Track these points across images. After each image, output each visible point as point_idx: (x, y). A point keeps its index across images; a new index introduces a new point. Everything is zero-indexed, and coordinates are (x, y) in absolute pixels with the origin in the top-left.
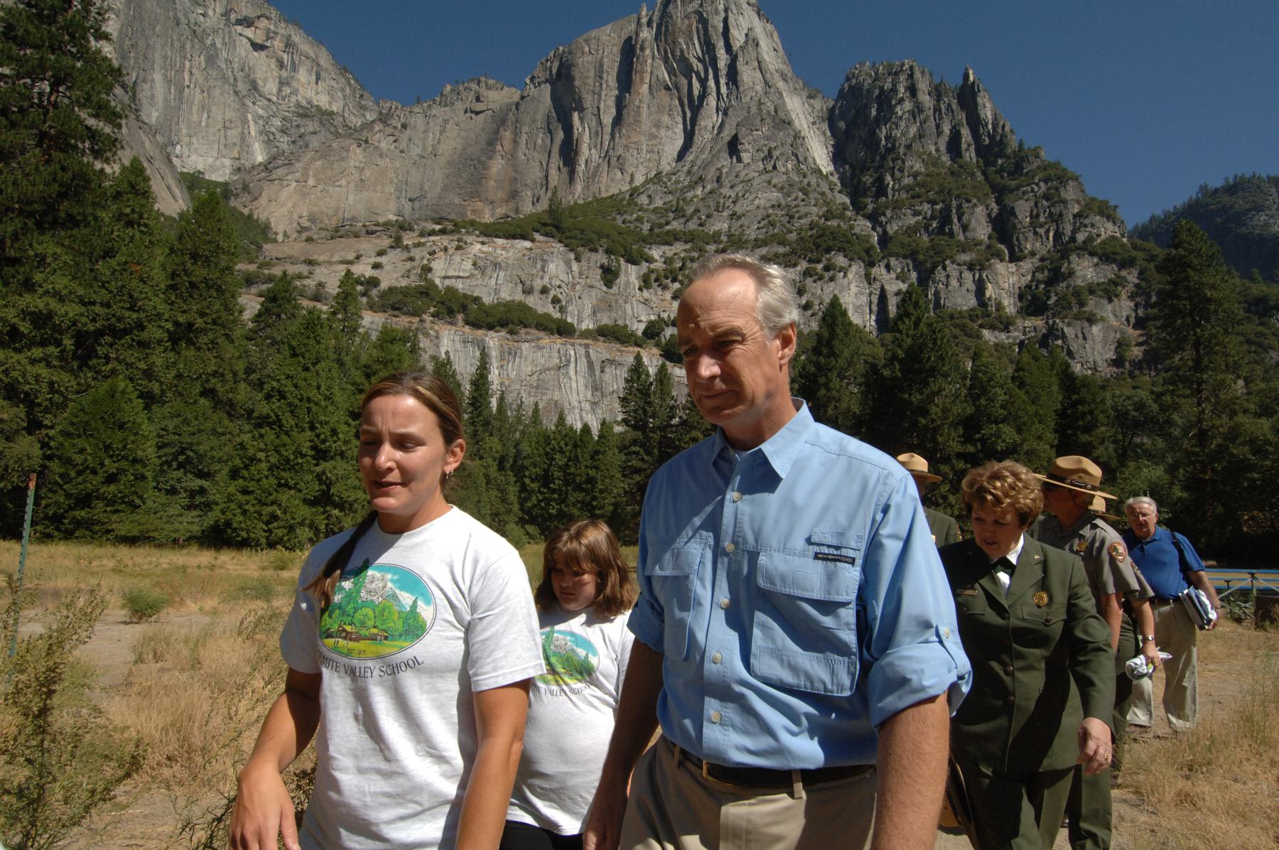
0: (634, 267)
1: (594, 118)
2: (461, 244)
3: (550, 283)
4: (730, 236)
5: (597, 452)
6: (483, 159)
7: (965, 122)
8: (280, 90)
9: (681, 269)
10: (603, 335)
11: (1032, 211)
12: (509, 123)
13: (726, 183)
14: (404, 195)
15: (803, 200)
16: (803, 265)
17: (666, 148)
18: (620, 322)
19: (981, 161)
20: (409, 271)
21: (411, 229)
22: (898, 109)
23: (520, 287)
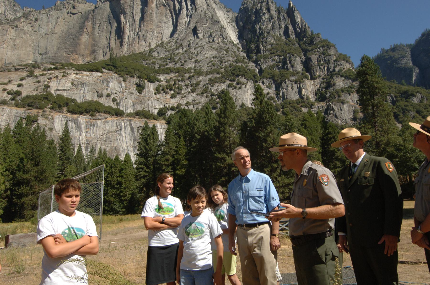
0: (152, 84)
2: (65, 74)
3: (111, 92)
4: (195, 70)
5: (122, 169)
6: (77, 35)
7: (290, 23)
9: (174, 85)
10: (138, 115)
11: (318, 59)
13: (193, 47)
14: (37, 52)
15: (226, 55)
16: (228, 82)
17: (165, 32)
18: (146, 109)
19: (297, 39)
20: (37, 87)
21: (39, 68)
22: (263, 17)
23: (96, 94)
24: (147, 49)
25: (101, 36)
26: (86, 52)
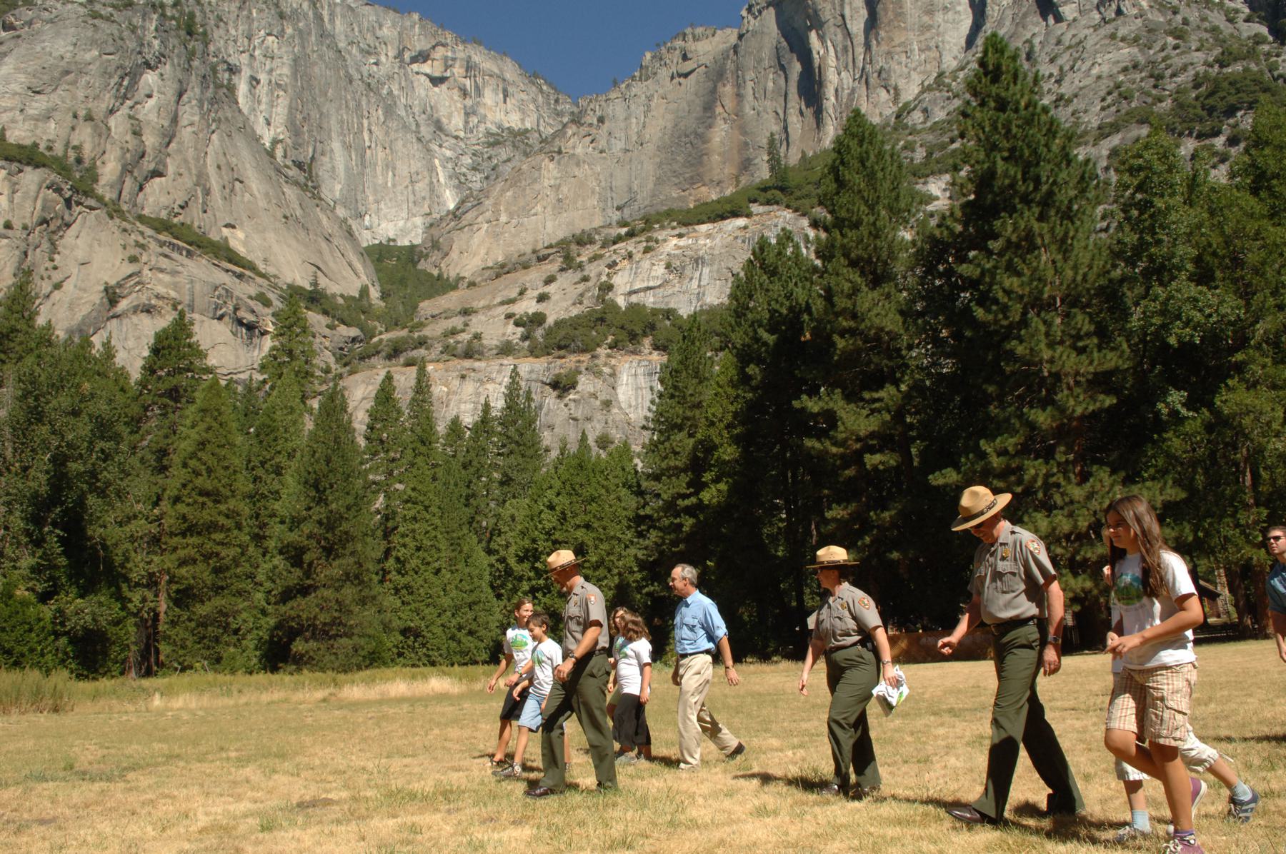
1: (839, 30)
2: (650, 244)
6: (700, 131)
8: (467, 122)
12: (729, 75)
13: (1043, 57)
15: (1176, 47)
17: (947, 38)
20: (582, 295)
21: (592, 242)
24: (890, 110)
25: (762, 114)
26: (726, 171)
